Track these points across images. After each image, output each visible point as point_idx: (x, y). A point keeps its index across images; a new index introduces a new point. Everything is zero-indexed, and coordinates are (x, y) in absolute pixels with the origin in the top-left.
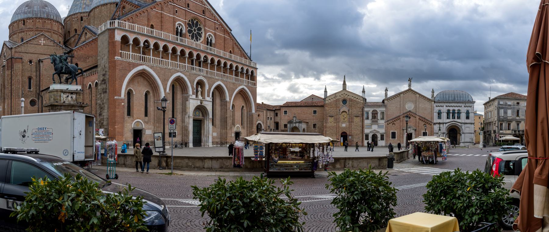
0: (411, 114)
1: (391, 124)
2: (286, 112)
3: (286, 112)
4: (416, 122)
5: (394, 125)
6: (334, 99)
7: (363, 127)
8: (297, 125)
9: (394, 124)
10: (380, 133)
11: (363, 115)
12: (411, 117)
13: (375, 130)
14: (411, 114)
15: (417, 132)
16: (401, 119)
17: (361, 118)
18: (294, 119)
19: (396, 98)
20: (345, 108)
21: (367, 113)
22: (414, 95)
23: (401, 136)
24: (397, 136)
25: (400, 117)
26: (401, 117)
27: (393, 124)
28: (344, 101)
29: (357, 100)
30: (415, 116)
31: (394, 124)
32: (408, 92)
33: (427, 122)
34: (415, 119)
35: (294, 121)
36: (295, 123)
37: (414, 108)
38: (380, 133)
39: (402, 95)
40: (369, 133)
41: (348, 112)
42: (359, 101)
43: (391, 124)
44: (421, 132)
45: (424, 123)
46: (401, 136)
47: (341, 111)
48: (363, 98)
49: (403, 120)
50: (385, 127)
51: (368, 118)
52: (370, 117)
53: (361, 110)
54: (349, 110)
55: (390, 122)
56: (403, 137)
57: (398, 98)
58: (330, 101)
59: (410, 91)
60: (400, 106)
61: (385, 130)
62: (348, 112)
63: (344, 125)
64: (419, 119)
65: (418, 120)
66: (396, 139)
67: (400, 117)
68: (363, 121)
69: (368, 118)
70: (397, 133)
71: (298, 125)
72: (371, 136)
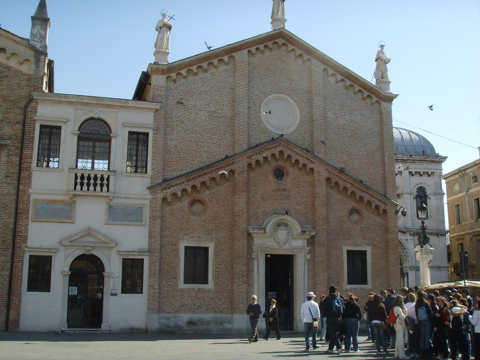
0: (287, 153)
1: (185, 203)
4: (314, 196)
5: (198, 207)
9: (201, 202)
10: (119, 253)
12: (290, 169)
13: (89, 232)
14: (287, 153)
15: (320, 250)
16: (240, 178)
17: (16, 159)
19: (212, 70)
22: (300, 61)
23: (240, 268)
24: (215, 272)
25: (235, 167)
26: (240, 164)
27: (193, 202)
30: (310, 165)
31: (201, 202)
32: (270, 44)
33: (367, 197)
34: (308, 178)
37: (302, 123)
38: (119, 253)
39: (241, 56)
40: (57, 250)
42: (13, 63)
43: (185, 203)
44: (341, 250)
45: (351, 204)
46: (240, 268)
48: (33, 48)
49: (248, 183)
50: (152, 218)
53: (16, 115)
55: (178, 190)
56: (249, 273)
57: (222, 67)
59: (280, 41)
60: (233, 107)
61: (151, 237)
64: (328, 179)
65: (321, 189)
66: (210, 285)
67: (235, 167)
70: (216, 254)
72: (67, 269)
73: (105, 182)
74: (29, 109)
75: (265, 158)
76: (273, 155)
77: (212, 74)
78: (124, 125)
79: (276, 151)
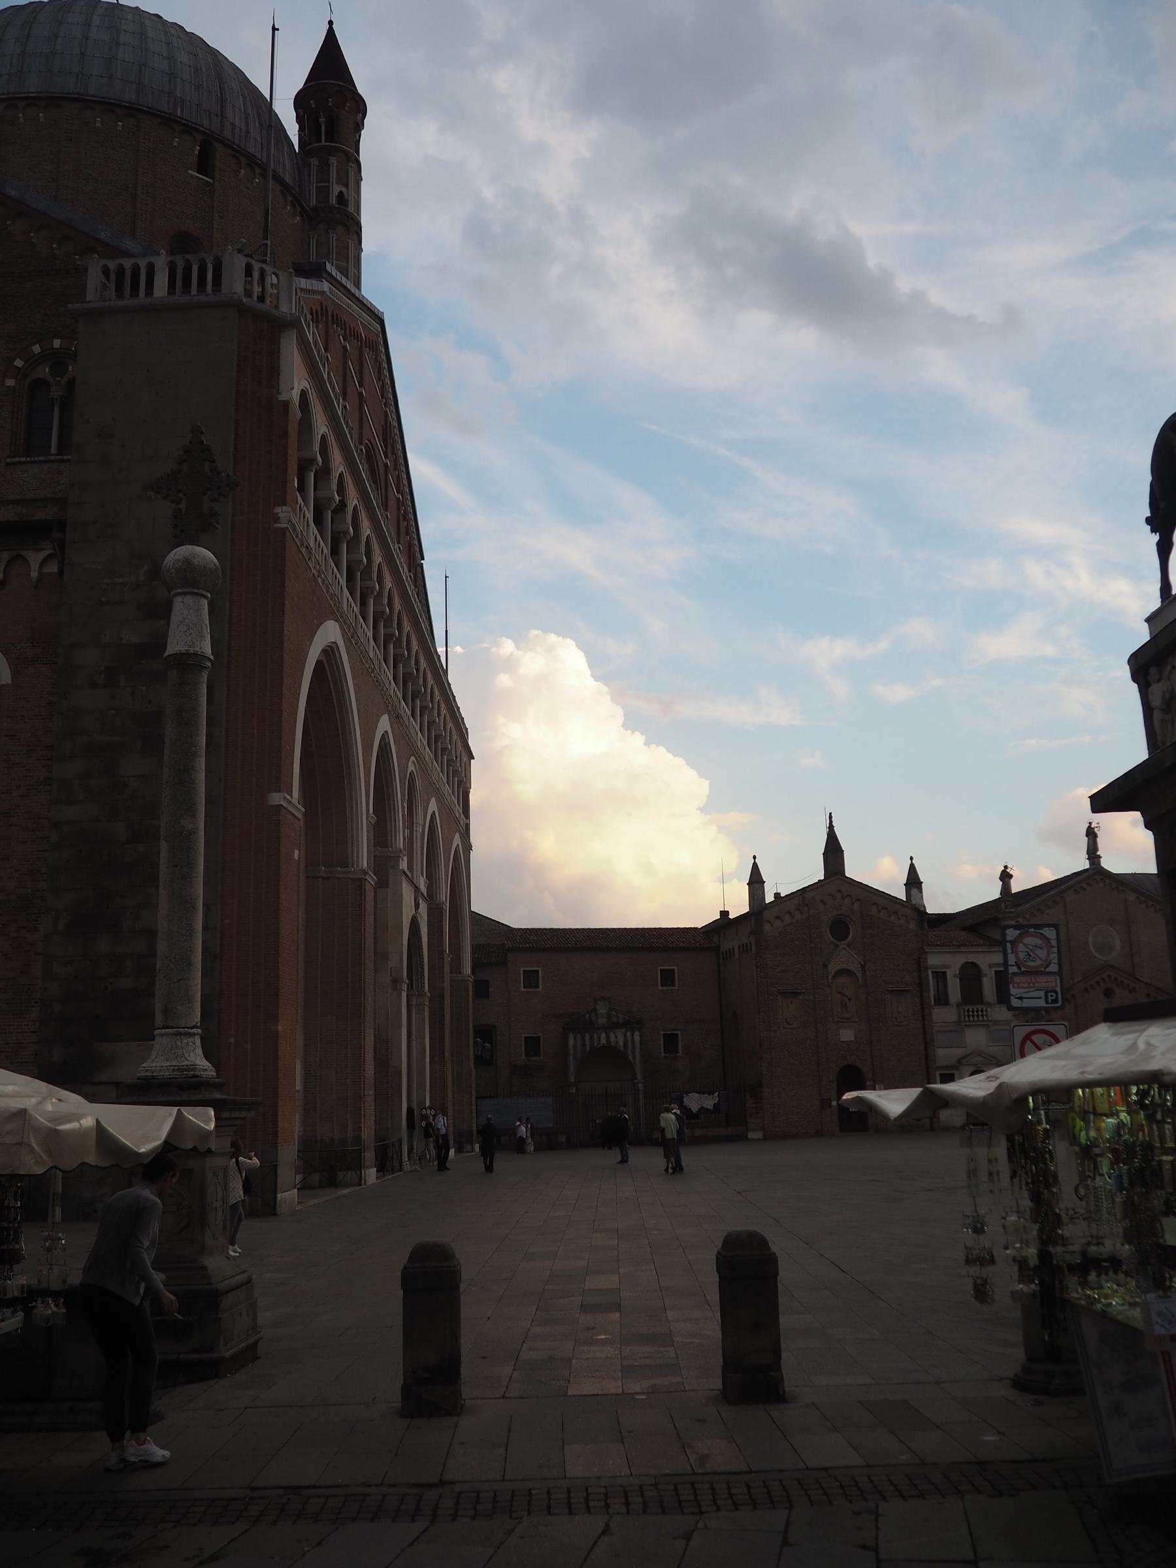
2: (531, 978)
3: (531, 978)
6: (798, 916)
7: (927, 1043)
8: (618, 1038)
11: (921, 985)
17: (917, 1000)
18: (602, 1009)
20: (845, 957)
21: (941, 976)
28: (840, 928)
29: (893, 918)
35: (602, 1021)
36: (610, 1028)
41: (859, 975)
47: (833, 968)
51: (942, 1000)
52: (954, 991)
54: (863, 967)
58: (778, 923)
62: (859, 975)
63: (847, 1035)
68: (923, 1012)
69: (942, 1000)
71: (621, 1040)
73: (985, 1013)
74: (922, 960)
75: (1098, 983)
76: (1103, 979)
77: (1047, 914)
78: (990, 966)
79: (1105, 976)
